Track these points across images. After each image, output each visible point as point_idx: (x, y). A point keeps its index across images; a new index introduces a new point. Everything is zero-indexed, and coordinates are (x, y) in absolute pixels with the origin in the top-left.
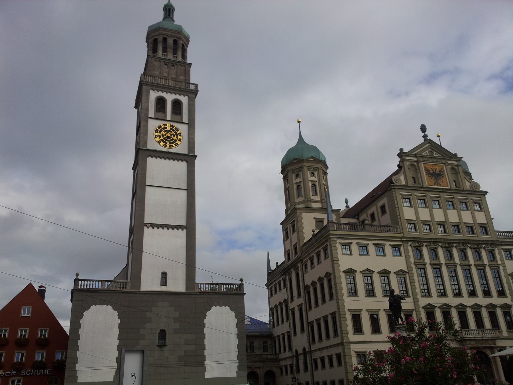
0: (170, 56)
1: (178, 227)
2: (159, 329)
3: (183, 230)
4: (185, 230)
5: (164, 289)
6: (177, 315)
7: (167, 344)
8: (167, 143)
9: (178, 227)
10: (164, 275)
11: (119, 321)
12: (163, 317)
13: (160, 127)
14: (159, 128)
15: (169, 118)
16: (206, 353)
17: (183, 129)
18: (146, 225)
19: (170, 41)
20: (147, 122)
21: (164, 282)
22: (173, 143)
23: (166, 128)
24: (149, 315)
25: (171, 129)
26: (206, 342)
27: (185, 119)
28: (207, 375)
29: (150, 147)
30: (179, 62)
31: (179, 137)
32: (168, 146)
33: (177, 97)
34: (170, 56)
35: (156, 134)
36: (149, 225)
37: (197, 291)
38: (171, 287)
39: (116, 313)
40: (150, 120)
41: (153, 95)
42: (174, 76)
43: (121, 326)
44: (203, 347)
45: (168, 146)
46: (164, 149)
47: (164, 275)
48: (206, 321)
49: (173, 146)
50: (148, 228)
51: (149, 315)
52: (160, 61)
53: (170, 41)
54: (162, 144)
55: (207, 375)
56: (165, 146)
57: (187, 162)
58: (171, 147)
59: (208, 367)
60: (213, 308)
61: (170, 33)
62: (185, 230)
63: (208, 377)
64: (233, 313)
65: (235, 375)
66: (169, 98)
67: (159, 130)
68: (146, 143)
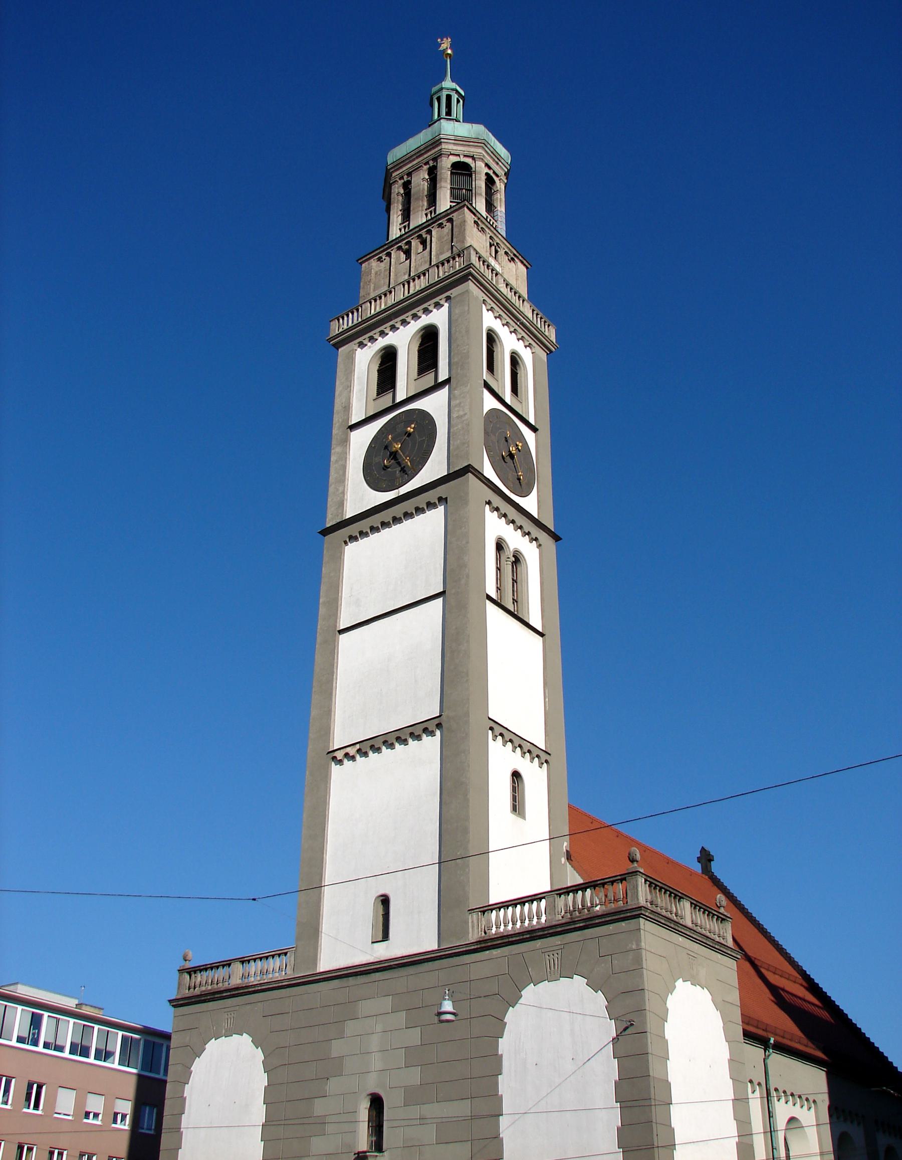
2: (365, 1094)
6: (414, 1037)
7: (385, 1147)
11: (262, 1080)
12: (375, 1050)
17: (435, 405)
24: (337, 1048)
27: (443, 375)
36: (339, 755)
37: (474, 935)
38: (399, 946)
39: (259, 1055)
48: (504, 1045)
60: (529, 993)
64: (600, 999)
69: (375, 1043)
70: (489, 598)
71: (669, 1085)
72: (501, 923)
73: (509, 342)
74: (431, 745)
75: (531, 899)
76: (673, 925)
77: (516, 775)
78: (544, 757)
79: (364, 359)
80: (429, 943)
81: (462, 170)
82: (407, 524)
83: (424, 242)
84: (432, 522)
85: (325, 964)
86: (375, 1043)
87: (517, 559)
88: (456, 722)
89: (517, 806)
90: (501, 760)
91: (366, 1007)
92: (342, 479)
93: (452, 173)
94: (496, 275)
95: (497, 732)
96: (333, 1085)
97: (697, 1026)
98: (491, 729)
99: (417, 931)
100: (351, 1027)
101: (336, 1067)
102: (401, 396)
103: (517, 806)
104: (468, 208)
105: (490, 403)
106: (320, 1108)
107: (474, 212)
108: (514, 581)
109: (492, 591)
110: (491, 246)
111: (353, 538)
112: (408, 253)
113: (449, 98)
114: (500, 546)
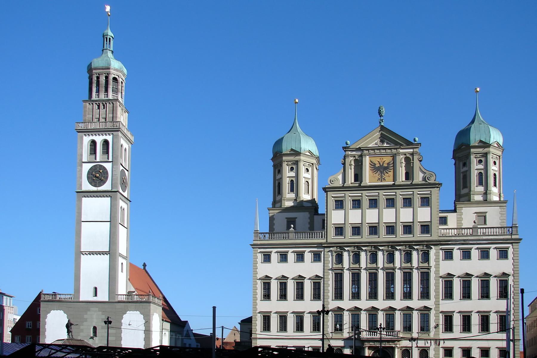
0: (102, 96)
1: (103, 253)
9: (103, 253)
15: (98, 160)
17: (108, 166)
18: (82, 253)
20: (81, 166)
22: (102, 182)
23: (96, 169)
24: (85, 316)
27: (110, 160)
29: (84, 189)
30: (109, 100)
33: (105, 137)
34: (102, 96)
36: (84, 253)
37: (116, 300)
38: (99, 298)
39: (66, 315)
40: (84, 164)
45: (98, 185)
47: (96, 288)
48: (123, 321)
51: (85, 316)
54: (93, 184)
56: (95, 186)
60: (128, 312)
66: (99, 139)
67: (91, 173)
68: (81, 185)
69: (94, 316)
72: (120, 298)
74: (107, 257)
76: (154, 303)
79: (87, 140)
81: (115, 79)
82: (100, 198)
83: (104, 105)
84: (107, 201)
85: (81, 299)
86: (94, 316)
88: (112, 252)
91: (92, 309)
92: (81, 177)
96: (85, 323)
99: (104, 296)
100: (89, 313)
101: (86, 320)
102: (98, 160)
106: (82, 327)
111: (85, 197)
112: (99, 108)
113: (110, 39)
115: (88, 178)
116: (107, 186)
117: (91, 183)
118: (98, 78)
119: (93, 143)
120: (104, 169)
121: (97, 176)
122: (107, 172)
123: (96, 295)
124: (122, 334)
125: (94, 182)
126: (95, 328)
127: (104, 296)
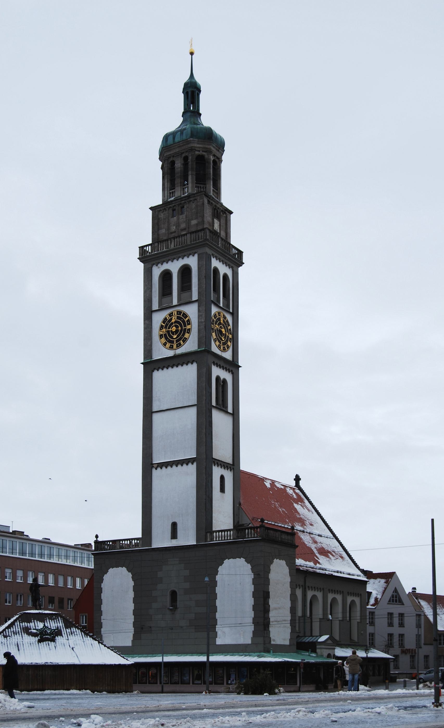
2: (170, 590)
3: (192, 464)
4: (195, 464)
5: (174, 543)
8: (172, 342)
10: (174, 526)
12: (173, 577)
13: (165, 320)
14: (164, 322)
15: (175, 302)
16: (218, 615)
19: (179, 164)
21: (174, 535)
23: (171, 319)
25: (178, 318)
26: (218, 603)
28: (219, 641)
31: (188, 327)
32: (175, 346)
35: (161, 333)
38: (181, 541)
41: (157, 272)
42: (183, 226)
43: (135, 589)
44: (214, 609)
45: (175, 346)
46: (170, 353)
47: (174, 526)
49: (180, 344)
50: (156, 469)
52: (165, 209)
53: (179, 164)
54: (168, 345)
55: (219, 641)
56: (171, 348)
57: (196, 362)
58: (179, 346)
59: (219, 633)
60: (226, 561)
61: (177, 150)
62: (195, 464)
63: (220, 644)
64: (249, 566)
65: (249, 642)
66: (174, 267)
70: (213, 406)
71: (269, 592)
73: (223, 269)
75: (227, 530)
77: (222, 478)
78: (232, 467)
80: (193, 542)
87: (225, 381)
89: (222, 490)
90: (217, 472)
93: (196, 163)
94: (218, 237)
95: (216, 463)
97: (279, 572)
98: (214, 462)
99: (188, 538)
103: (222, 490)
104: (205, 195)
105: (214, 310)
107: (207, 196)
108: (223, 392)
109: (214, 403)
110: (215, 209)
114: (218, 378)
115: (161, 336)
116: (191, 345)
117: (165, 344)
118: (173, 163)
119: (166, 276)
120: (185, 315)
121: (175, 331)
122: (189, 322)
123: (174, 535)
124: (217, 601)
125: (170, 341)
126: (174, 594)
127: (188, 538)
